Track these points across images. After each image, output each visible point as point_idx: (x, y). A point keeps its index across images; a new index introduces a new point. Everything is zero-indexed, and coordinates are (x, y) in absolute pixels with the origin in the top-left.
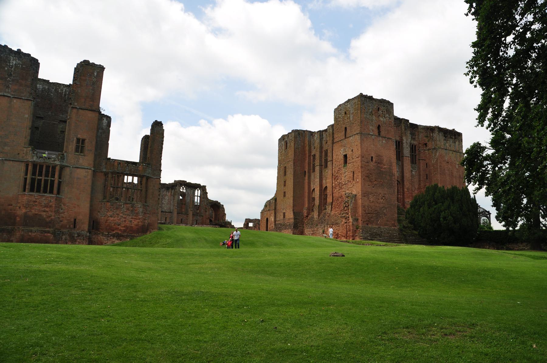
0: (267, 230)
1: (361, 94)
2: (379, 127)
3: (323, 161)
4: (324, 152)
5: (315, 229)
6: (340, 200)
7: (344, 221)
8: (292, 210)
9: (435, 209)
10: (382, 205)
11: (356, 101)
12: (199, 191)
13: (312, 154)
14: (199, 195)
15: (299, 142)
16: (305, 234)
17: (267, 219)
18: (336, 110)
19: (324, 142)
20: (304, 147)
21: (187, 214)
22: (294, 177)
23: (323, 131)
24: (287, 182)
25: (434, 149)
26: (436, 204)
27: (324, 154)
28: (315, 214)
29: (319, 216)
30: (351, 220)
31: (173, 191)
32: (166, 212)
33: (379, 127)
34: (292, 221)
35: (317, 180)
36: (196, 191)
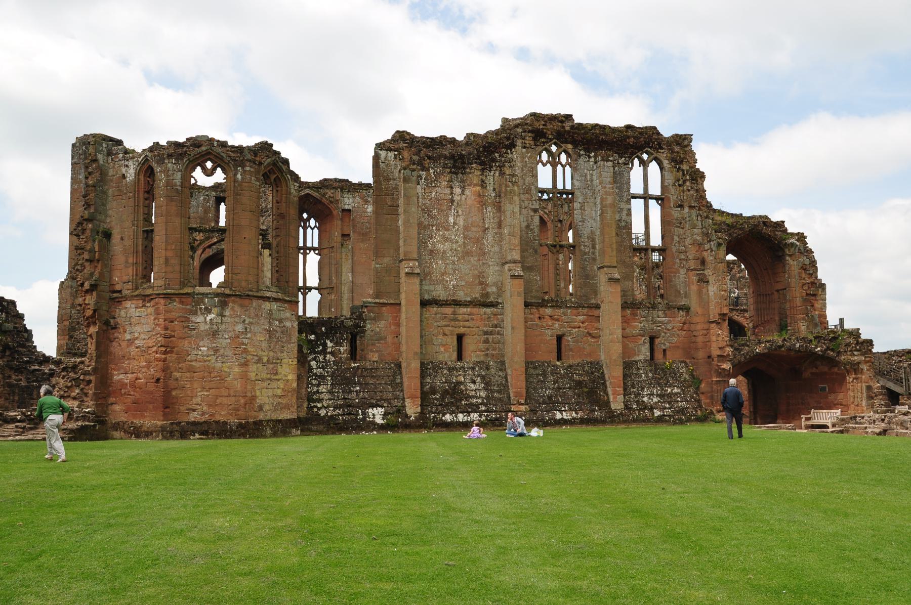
12: (654, 167)
14: (655, 189)
21: (588, 304)
31: (492, 178)
32: (457, 303)
36: (636, 172)
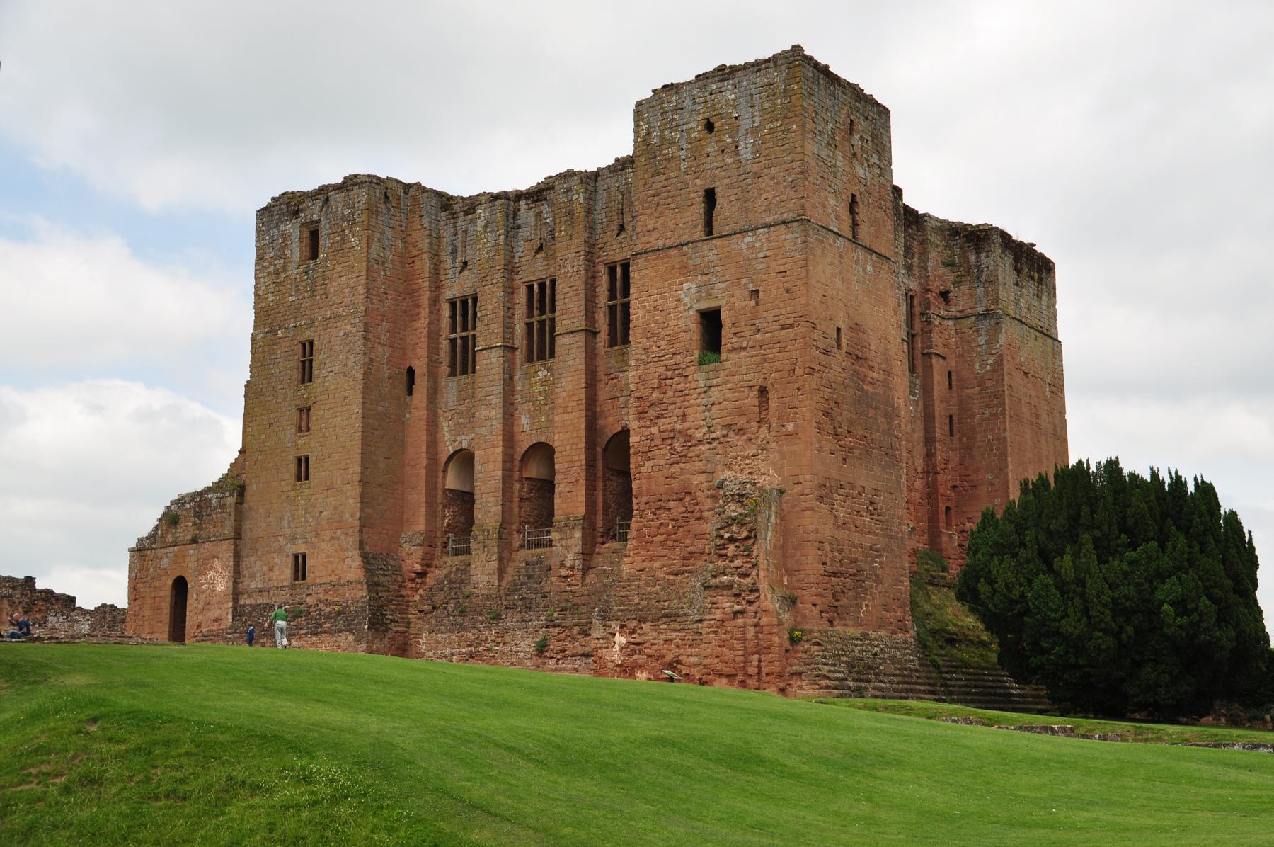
0: (178, 633)
1: (797, 49)
2: (853, 202)
3: (520, 328)
4: (523, 291)
5: (490, 635)
6: (677, 508)
7: (727, 604)
8: (352, 542)
9: (1131, 563)
10: (868, 540)
11: (778, 76)
13: (448, 295)
15: (389, 232)
16: (420, 655)
17: (180, 585)
18: (641, 109)
19: (522, 250)
20: (407, 260)
22: (366, 390)
23: (519, 196)
24: (316, 414)
25: (986, 315)
26: (1133, 546)
27: (521, 297)
28: (482, 572)
29: (501, 572)
30: (769, 600)
33: (853, 202)
34: (362, 593)
35: (491, 414)
